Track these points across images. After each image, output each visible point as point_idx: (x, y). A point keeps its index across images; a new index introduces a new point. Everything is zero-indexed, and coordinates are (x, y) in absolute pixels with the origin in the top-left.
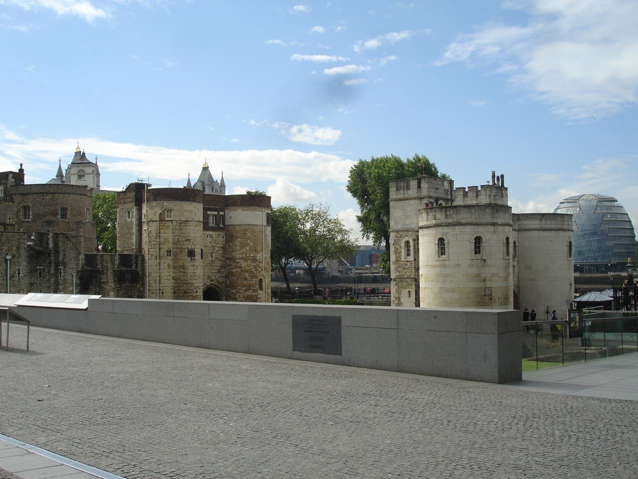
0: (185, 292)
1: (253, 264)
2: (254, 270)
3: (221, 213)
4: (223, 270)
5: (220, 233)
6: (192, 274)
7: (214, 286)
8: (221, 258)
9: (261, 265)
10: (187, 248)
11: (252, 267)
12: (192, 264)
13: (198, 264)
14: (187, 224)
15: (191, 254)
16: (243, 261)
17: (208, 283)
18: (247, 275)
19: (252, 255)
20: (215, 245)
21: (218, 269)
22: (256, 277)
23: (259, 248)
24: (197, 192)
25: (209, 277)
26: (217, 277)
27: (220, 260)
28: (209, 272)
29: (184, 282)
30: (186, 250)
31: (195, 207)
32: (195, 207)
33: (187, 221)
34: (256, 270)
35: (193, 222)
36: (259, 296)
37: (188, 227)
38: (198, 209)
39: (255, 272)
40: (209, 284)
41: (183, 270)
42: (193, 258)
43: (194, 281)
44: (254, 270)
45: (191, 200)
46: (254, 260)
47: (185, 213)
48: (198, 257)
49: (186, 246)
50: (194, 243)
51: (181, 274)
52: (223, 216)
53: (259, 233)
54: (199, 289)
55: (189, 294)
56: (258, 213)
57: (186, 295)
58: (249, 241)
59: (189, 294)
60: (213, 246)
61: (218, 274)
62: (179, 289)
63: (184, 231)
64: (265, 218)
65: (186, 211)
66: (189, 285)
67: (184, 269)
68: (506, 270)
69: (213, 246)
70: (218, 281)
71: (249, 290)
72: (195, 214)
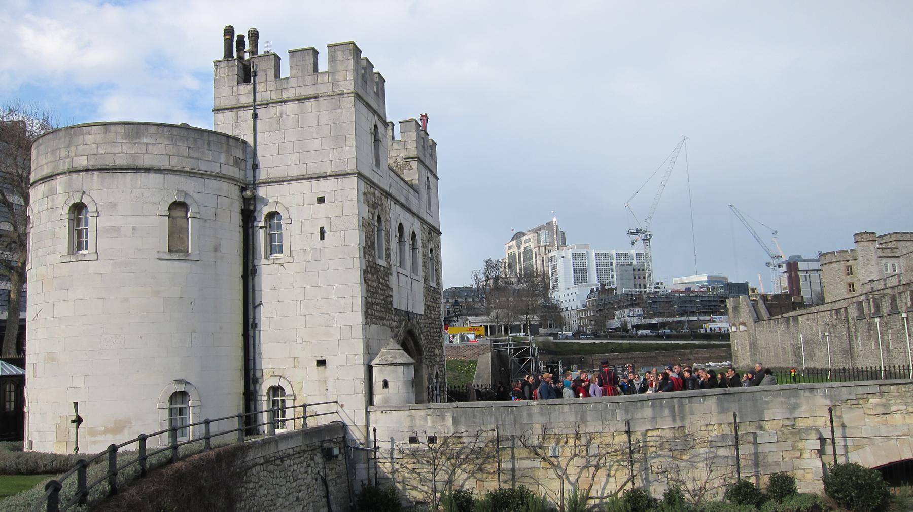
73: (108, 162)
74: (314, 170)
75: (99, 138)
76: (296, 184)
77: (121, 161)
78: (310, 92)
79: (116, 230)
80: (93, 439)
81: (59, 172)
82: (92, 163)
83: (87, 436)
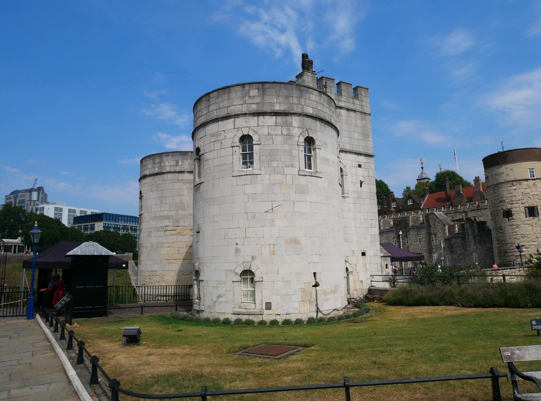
0: (506, 252)
10: (502, 209)
12: (511, 224)
13: (519, 223)
14: (500, 187)
24: (506, 153)
29: (503, 242)
31: (506, 168)
37: (502, 189)
38: (511, 169)
41: (501, 231)
45: (500, 162)
51: (501, 235)
54: (527, 248)
55: (510, 254)
57: (506, 255)
59: (510, 254)
62: (501, 250)
63: (497, 194)
72: (508, 175)
73: (322, 115)
74: (355, 149)
75: (318, 98)
76: (348, 155)
77: (327, 118)
78: (351, 106)
79: (326, 160)
80: (326, 298)
81: (294, 112)
82: (315, 114)
83: (323, 296)
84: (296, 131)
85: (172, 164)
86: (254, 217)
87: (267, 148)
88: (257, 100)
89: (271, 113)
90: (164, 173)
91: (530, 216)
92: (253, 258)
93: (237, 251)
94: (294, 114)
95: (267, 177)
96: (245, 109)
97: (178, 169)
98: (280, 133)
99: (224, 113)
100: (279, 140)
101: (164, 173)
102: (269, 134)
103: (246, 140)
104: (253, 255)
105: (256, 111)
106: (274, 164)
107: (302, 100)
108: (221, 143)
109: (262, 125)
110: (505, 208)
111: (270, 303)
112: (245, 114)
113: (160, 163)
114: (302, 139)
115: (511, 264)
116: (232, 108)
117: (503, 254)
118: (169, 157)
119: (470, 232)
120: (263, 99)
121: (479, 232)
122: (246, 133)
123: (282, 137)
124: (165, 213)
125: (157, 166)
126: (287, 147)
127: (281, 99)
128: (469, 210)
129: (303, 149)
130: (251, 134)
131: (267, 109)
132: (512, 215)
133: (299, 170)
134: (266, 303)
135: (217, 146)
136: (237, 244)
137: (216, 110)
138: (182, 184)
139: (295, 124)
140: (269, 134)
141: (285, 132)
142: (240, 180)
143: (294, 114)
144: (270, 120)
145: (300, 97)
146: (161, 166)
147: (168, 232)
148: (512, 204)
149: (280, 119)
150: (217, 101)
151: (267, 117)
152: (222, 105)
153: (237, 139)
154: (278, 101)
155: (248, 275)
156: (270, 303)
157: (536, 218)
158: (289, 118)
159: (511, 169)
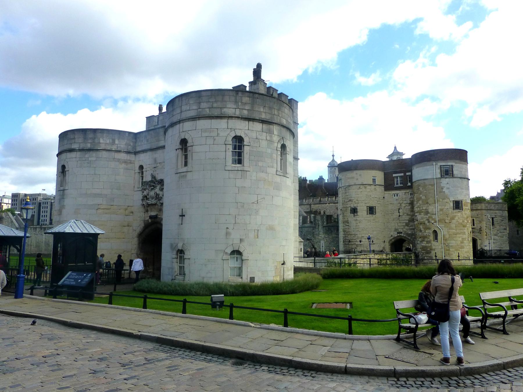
0: (350, 241)
1: (426, 216)
2: (426, 222)
3: (407, 174)
4: (411, 224)
5: (408, 191)
6: (355, 227)
7: (403, 238)
8: (409, 213)
9: (434, 217)
11: (424, 220)
15: (354, 211)
16: (418, 214)
17: (395, 235)
18: (421, 227)
19: (424, 208)
20: (401, 202)
21: (406, 223)
22: (429, 228)
23: (431, 200)
25: (396, 230)
26: (405, 230)
27: (408, 215)
28: (397, 225)
30: (350, 209)
31: (357, 174)
32: (357, 174)
33: (349, 186)
34: (429, 222)
35: (354, 186)
36: (433, 247)
37: (350, 191)
38: (360, 175)
39: (428, 224)
40: (396, 236)
41: (348, 224)
42: (355, 214)
43: (358, 233)
44: (426, 222)
46: (427, 213)
47: (348, 180)
48: (362, 211)
49: (349, 206)
50: (356, 202)
52: (411, 177)
53: (430, 187)
55: (353, 243)
56: (428, 167)
58: (421, 195)
59: (353, 243)
60: (399, 203)
61: (406, 227)
64: (438, 171)
65: (349, 178)
66: (352, 236)
67: (348, 223)
68: (60, 202)
69: (399, 203)
70: (408, 234)
71: (424, 241)
72: (357, 179)
84: (276, 138)
85: (108, 142)
86: (243, 207)
87: (255, 150)
88: (247, 107)
89: (259, 120)
90: (97, 150)
91: (370, 213)
92: (241, 240)
93: (227, 234)
94: (276, 123)
95: (255, 174)
96: (238, 113)
97: (114, 148)
98: (265, 138)
99: (216, 113)
100: (264, 144)
101: (97, 150)
102: (257, 138)
103: (238, 141)
104: (242, 238)
105: (247, 117)
106: (260, 164)
107: (280, 112)
108: (214, 140)
109: (252, 129)
110: (352, 206)
111: (254, 278)
112: (238, 117)
113: (94, 139)
114: (279, 146)
115: (352, 251)
116: (225, 110)
117: (347, 243)
118: (105, 135)
119: (320, 223)
120: (252, 107)
121: (327, 223)
122: (238, 134)
123: (266, 142)
124: (98, 191)
125: (90, 141)
126: (269, 151)
127: (267, 110)
128: (313, 203)
129: (280, 153)
130: (243, 136)
131: (256, 116)
132: (357, 212)
133: (277, 171)
134: (250, 278)
135: (210, 141)
136: (227, 228)
137: (209, 108)
138: (117, 163)
139: (276, 132)
140: (257, 138)
141: (268, 138)
142: (232, 175)
143: (276, 123)
144: (258, 126)
145: (279, 110)
146: (94, 142)
147: (101, 211)
148: (358, 203)
149: (265, 126)
150: (210, 100)
151: (255, 123)
152: (215, 105)
153: (230, 139)
154: (264, 111)
155: (237, 253)
156: (254, 278)
157: (374, 216)
158: (271, 126)
159: (360, 175)
